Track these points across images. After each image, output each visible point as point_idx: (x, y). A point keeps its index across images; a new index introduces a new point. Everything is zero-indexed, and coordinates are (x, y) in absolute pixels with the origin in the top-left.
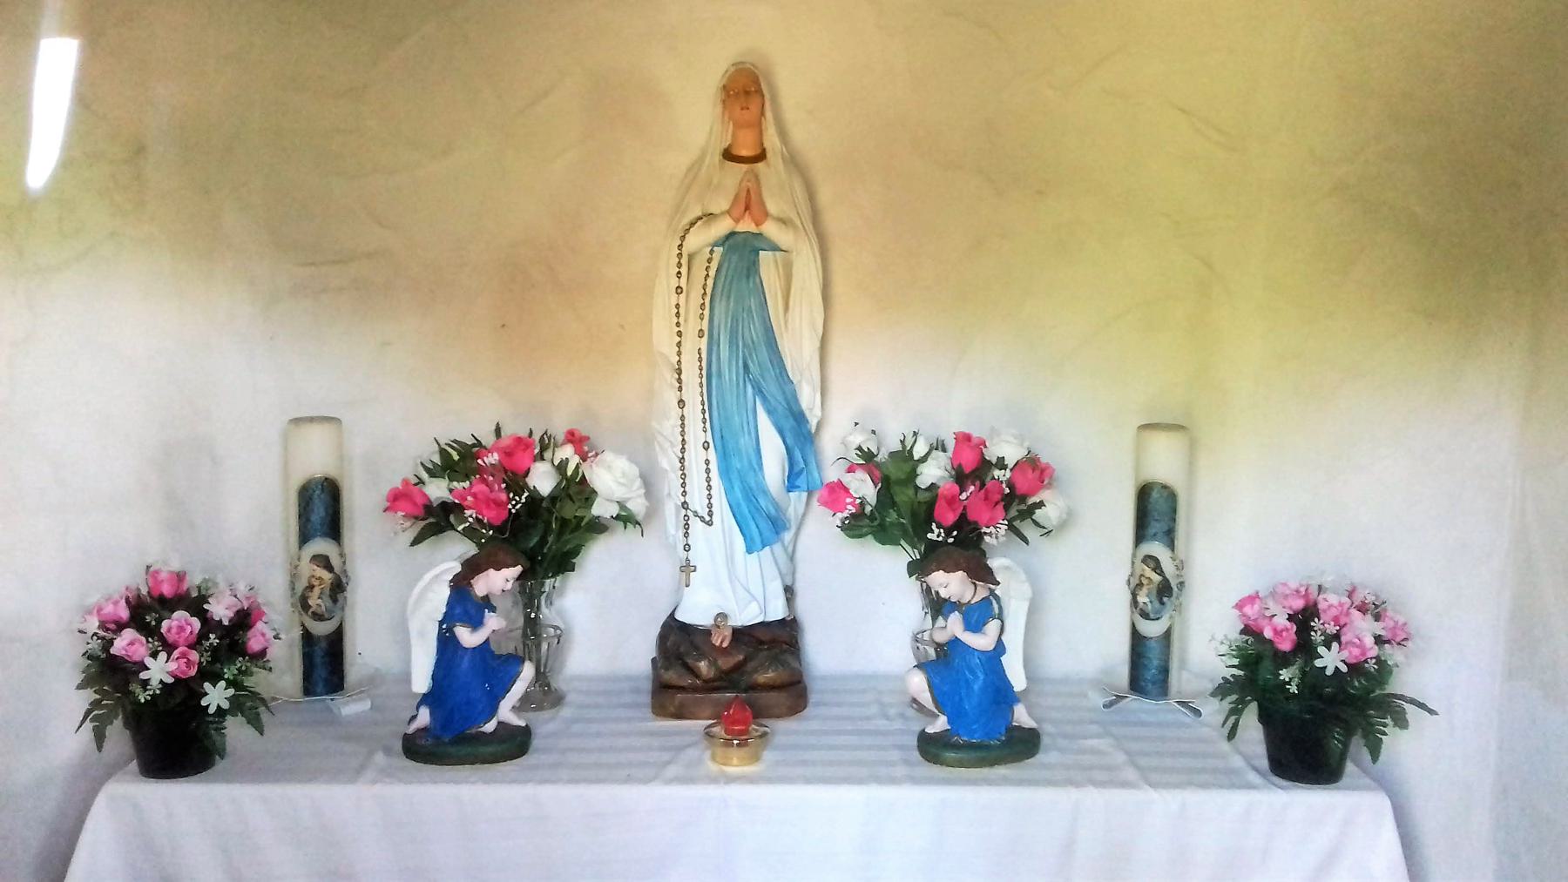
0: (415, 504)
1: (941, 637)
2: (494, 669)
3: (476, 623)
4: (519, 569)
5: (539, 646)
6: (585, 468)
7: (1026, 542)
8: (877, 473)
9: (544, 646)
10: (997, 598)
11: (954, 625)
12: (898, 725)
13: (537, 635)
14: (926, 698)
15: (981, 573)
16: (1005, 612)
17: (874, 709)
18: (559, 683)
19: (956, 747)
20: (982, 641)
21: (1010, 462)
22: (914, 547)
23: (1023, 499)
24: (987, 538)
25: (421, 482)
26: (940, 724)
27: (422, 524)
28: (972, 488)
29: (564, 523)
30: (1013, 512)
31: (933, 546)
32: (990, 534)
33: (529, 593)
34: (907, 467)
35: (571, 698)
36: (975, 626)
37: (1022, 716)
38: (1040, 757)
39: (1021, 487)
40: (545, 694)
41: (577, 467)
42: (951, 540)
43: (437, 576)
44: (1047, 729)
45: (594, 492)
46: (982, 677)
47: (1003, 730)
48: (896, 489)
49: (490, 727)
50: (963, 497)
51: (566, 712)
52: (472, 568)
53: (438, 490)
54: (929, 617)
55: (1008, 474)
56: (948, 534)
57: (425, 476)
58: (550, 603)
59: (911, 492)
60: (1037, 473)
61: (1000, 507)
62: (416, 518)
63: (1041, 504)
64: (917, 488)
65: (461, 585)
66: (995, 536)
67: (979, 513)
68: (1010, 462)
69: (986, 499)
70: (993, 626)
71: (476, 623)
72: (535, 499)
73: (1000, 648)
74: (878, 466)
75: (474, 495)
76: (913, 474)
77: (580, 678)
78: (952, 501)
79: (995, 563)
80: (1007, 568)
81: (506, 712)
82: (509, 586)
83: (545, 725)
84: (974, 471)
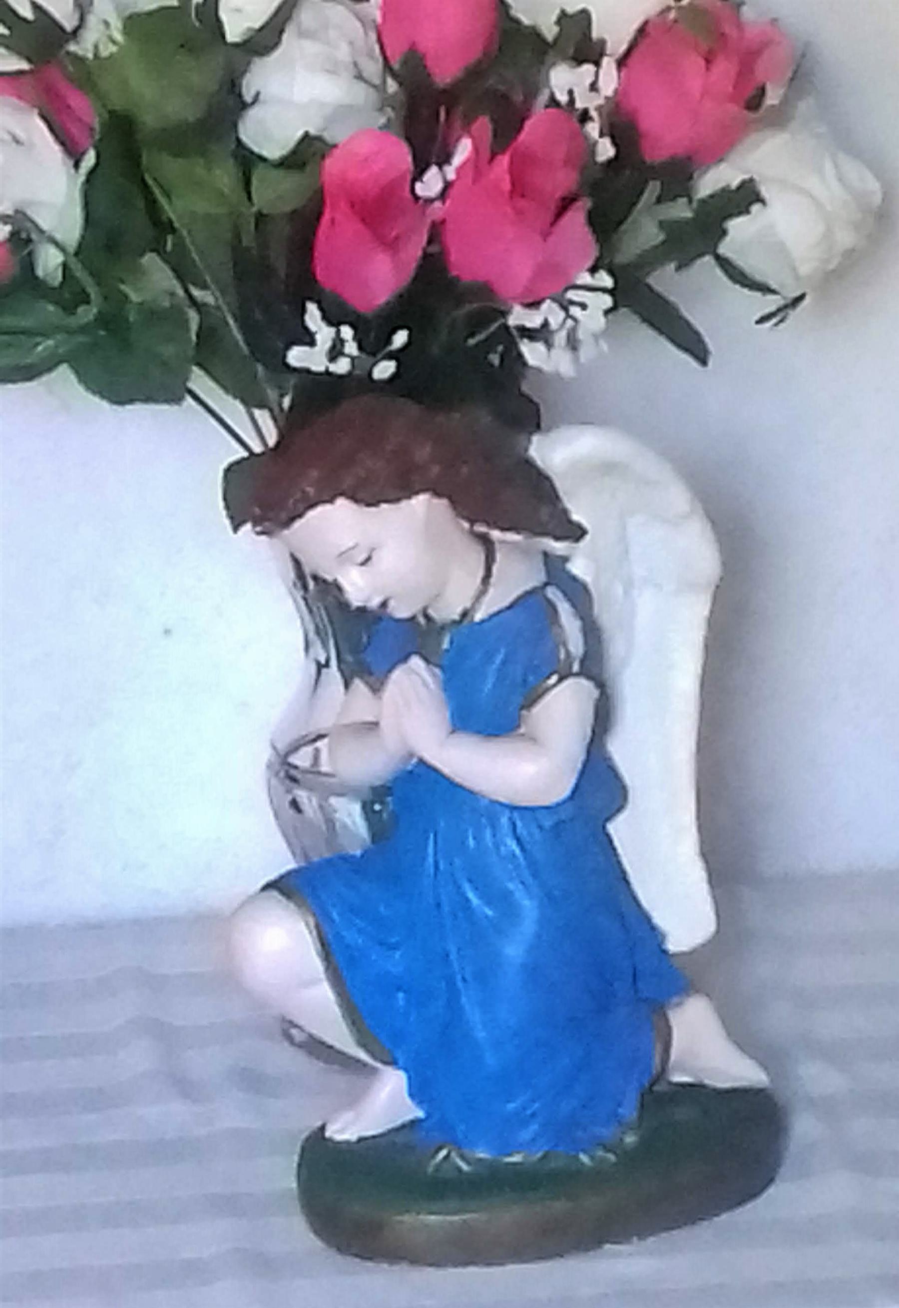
1: (367, 764)
7: (698, 351)
8: (89, 113)
10: (579, 594)
11: (411, 713)
12: (232, 1113)
14: (320, 1006)
15: (507, 496)
16: (616, 648)
17: (138, 1058)
19: (444, 1189)
20: (524, 771)
21: (615, 27)
22: (252, 400)
23: (678, 176)
24: (532, 353)
26: (385, 1103)
28: (463, 150)
30: (644, 231)
31: (320, 391)
32: (542, 334)
34: (203, 76)
36: (491, 711)
37: (702, 1046)
38: (780, 1199)
39: (666, 130)
42: (384, 369)
44: (815, 1078)
46: (528, 906)
47: (629, 1111)
48: (164, 167)
50: (431, 184)
54: (333, 672)
55: (609, 79)
56: (373, 342)
59: (225, 177)
60: (725, 69)
61: (576, 220)
63: (746, 197)
64: (247, 161)
66: (571, 334)
67: (494, 253)
68: (615, 27)
69: (519, 188)
70: (564, 707)
73: (600, 785)
74: (86, 74)
76: (231, 103)
78: (380, 210)
79: (557, 452)
80: (608, 468)
84: (475, 73)
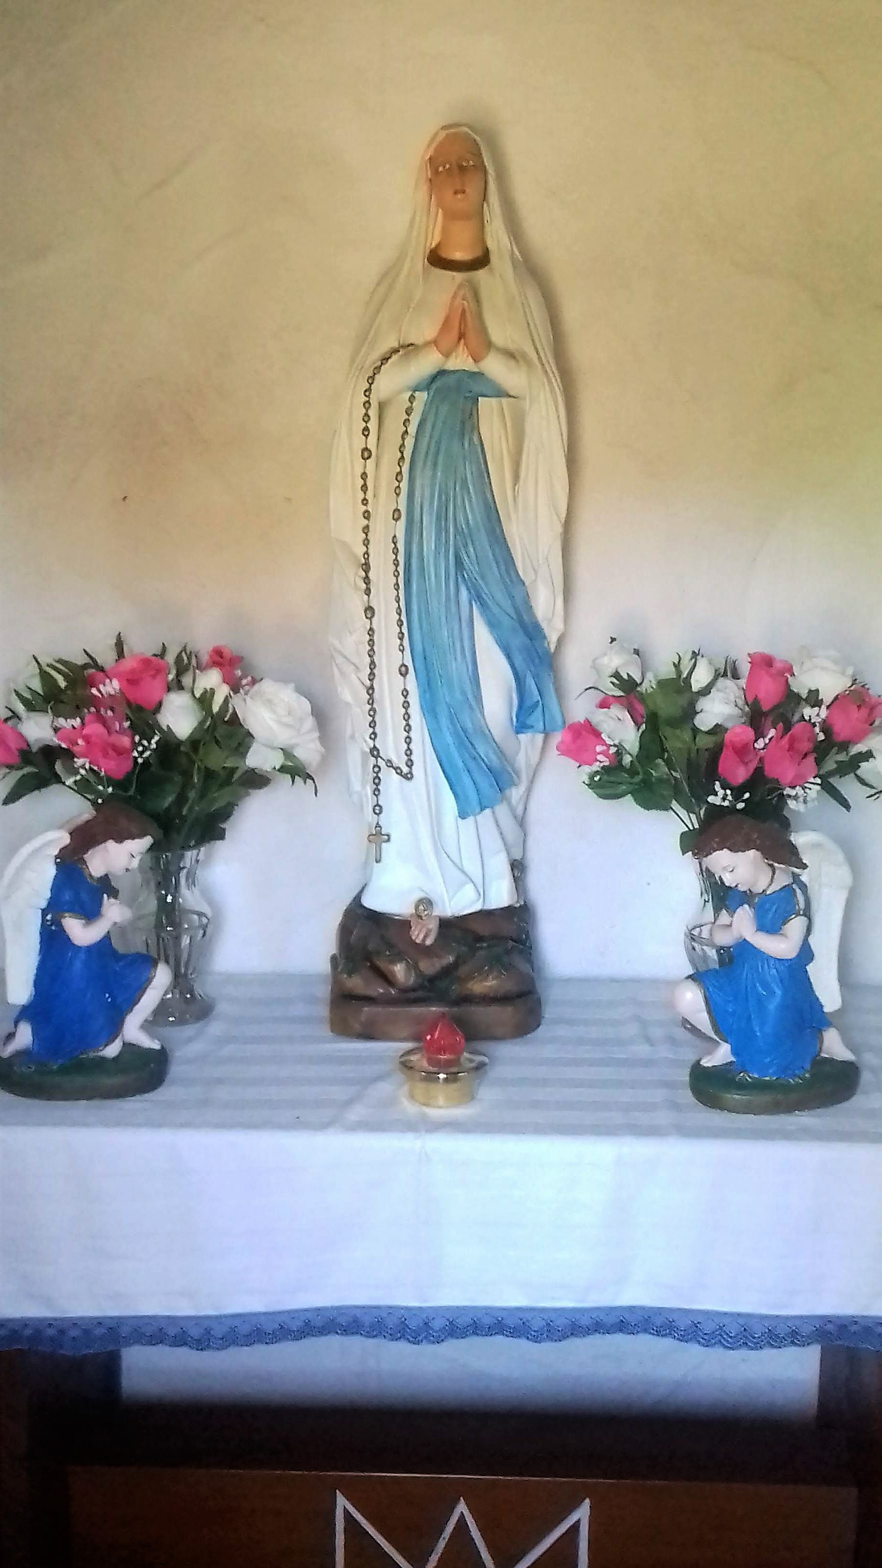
0: (8, 748)
1: (724, 939)
2: (115, 973)
3: (91, 914)
4: (148, 841)
5: (177, 939)
7: (846, 804)
8: (641, 709)
9: (185, 941)
10: (804, 887)
11: (742, 924)
12: (664, 1052)
13: (176, 925)
14: (703, 1020)
15: (781, 852)
16: (814, 906)
17: (632, 1030)
18: (203, 988)
19: (742, 1087)
20: (780, 946)
21: (827, 696)
22: (689, 810)
23: (844, 746)
24: (792, 804)
25: (15, 716)
26: (722, 1055)
27: (17, 775)
28: (772, 733)
29: (209, 775)
30: (830, 765)
31: (715, 812)
32: (796, 797)
33: (163, 873)
34: (683, 701)
35: (222, 1007)
36: (771, 924)
37: (833, 1045)
38: (858, 1101)
39: (842, 730)
40: (189, 1004)
41: (226, 701)
42: (740, 806)
43: (36, 851)
44: (869, 1059)
45: (249, 735)
46: (779, 992)
47: (808, 1066)
48: (666, 731)
49: (112, 1050)
50: (760, 744)
51: (215, 1028)
52: (84, 838)
53: (38, 729)
54: (710, 905)
55: (824, 713)
56: (737, 797)
57: (20, 708)
58: (192, 880)
59: (687, 736)
60: (864, 712)
61: (811, 759)
62: (10, 767)
63: (868, 755)
64: (695, 731)
65: (70, 863)
67: (782, 769)
68: (827, 696)
69: (791, 748)
70: (796, 926)
71: (91, 914)
73: (806, 954)
74: (642, 698)
75: (87, 739)
76: (691, 712)
77: (231, 979)
78: (743, 751)
79: (800, 839)
80: (817, 846)
81: (134, 1030)
82: (135, 863)
83: (190, 1046)
84: (776, 707)
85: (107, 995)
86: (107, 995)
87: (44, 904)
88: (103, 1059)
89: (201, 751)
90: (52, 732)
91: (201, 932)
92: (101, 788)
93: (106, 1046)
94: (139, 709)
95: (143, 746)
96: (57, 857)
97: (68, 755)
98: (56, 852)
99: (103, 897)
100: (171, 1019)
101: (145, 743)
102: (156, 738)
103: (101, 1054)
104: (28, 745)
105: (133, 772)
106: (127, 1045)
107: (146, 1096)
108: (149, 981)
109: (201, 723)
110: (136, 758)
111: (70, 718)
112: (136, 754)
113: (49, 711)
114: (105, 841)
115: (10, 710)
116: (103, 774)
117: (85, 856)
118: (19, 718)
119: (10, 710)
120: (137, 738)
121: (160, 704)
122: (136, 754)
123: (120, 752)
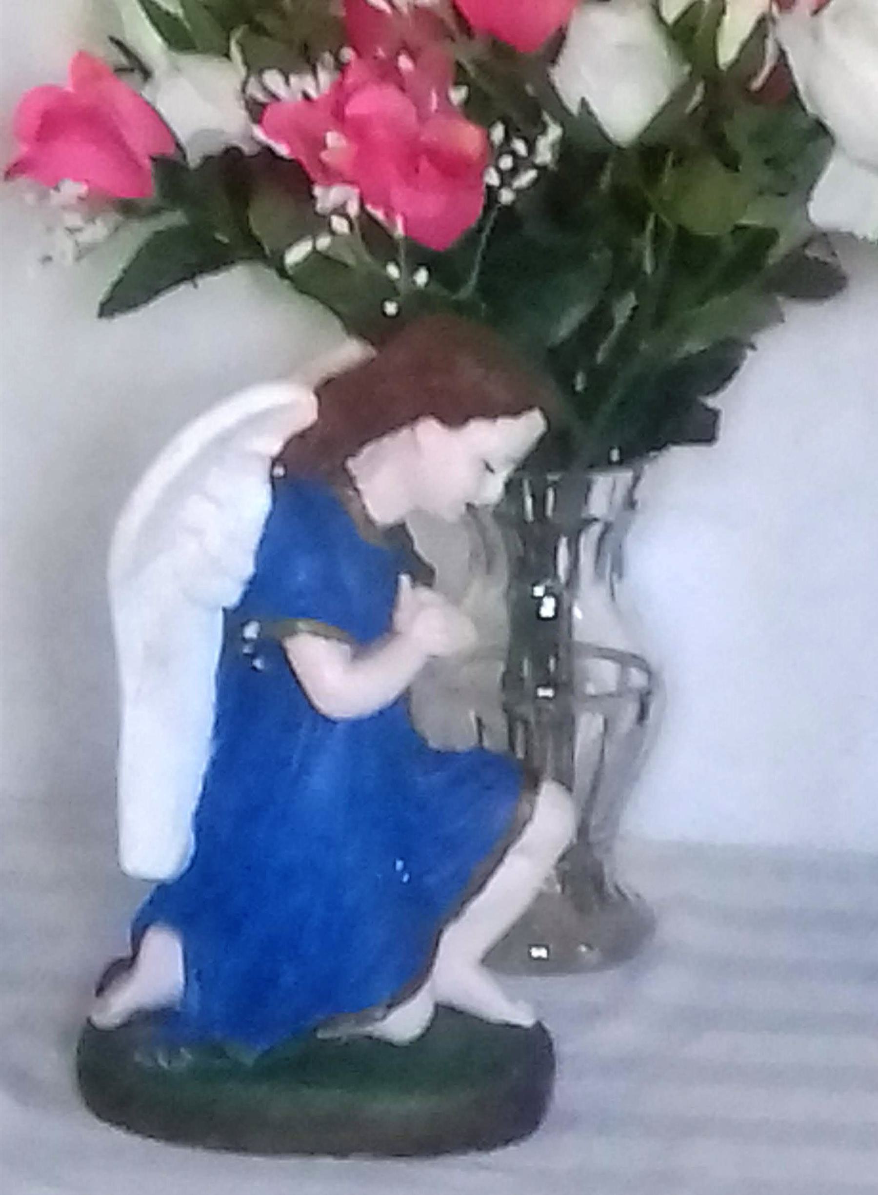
0: (129, 158)
2: (430, 804)
3: (366, 627)
4: (528, 427)
5: (565, 727)
6: (790, 33)
9: (588, 727)
13: (564, 686)
18: (631, 872)
25: (137, 67)
27: (139, 232)
29: (689, 254)
33: (533, 531)
35: (676, 929)
40: (593, 918)
41: (763, 25)
43: (223, 441)
45: (820, 130)
49: (405, 1022)
51: (665, 985)
52: (355, 413)
53: (203, 103)
57: (150, 43)
58: (613, 561)
62: (129, 209)
65: (309, 483)
71: (366, 627)
72: (586, 147)
75: (357, 130)
77: (691, 855)
81: (461, 971)
82: (493, 490)
83: (598, 1029)
85: (399, 864)
86: (399, 864)
87: (232, 594)
88: (386, 1045)
89: (668, 177)
90: (242, 114)
91: (631, 710)
92: (393, 271)
93: (390, 1006)
94: (502, 50)
95: (514, 154)
96: (275, 461)
97: (294, 180)
98: (275, 447)
99: (397, 582)
100: (536, 953)
101: (520, 147)
102: (554, 132)
103: (369, 1029)
104: (178, 145)
105: (480, 230)
106: (445, 1012)
107: (498, 1155)
108: (514, 830)
109: (679, 96)
110: (492, 193)
111: (299, 72)
112: (492, 178)
113: (235, 50)
114: (413, 419)
115: (119, 44)
116: (399, 231)
117: (351, 464)
118: (147, 74)
119: (119, 44)
120: (498, 133)
121: (559, 39)
122: (492, 178)
123: (455, 169)
